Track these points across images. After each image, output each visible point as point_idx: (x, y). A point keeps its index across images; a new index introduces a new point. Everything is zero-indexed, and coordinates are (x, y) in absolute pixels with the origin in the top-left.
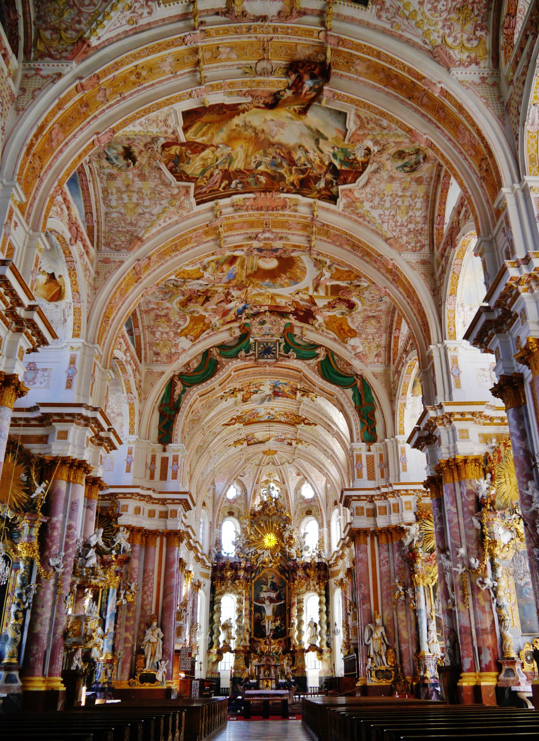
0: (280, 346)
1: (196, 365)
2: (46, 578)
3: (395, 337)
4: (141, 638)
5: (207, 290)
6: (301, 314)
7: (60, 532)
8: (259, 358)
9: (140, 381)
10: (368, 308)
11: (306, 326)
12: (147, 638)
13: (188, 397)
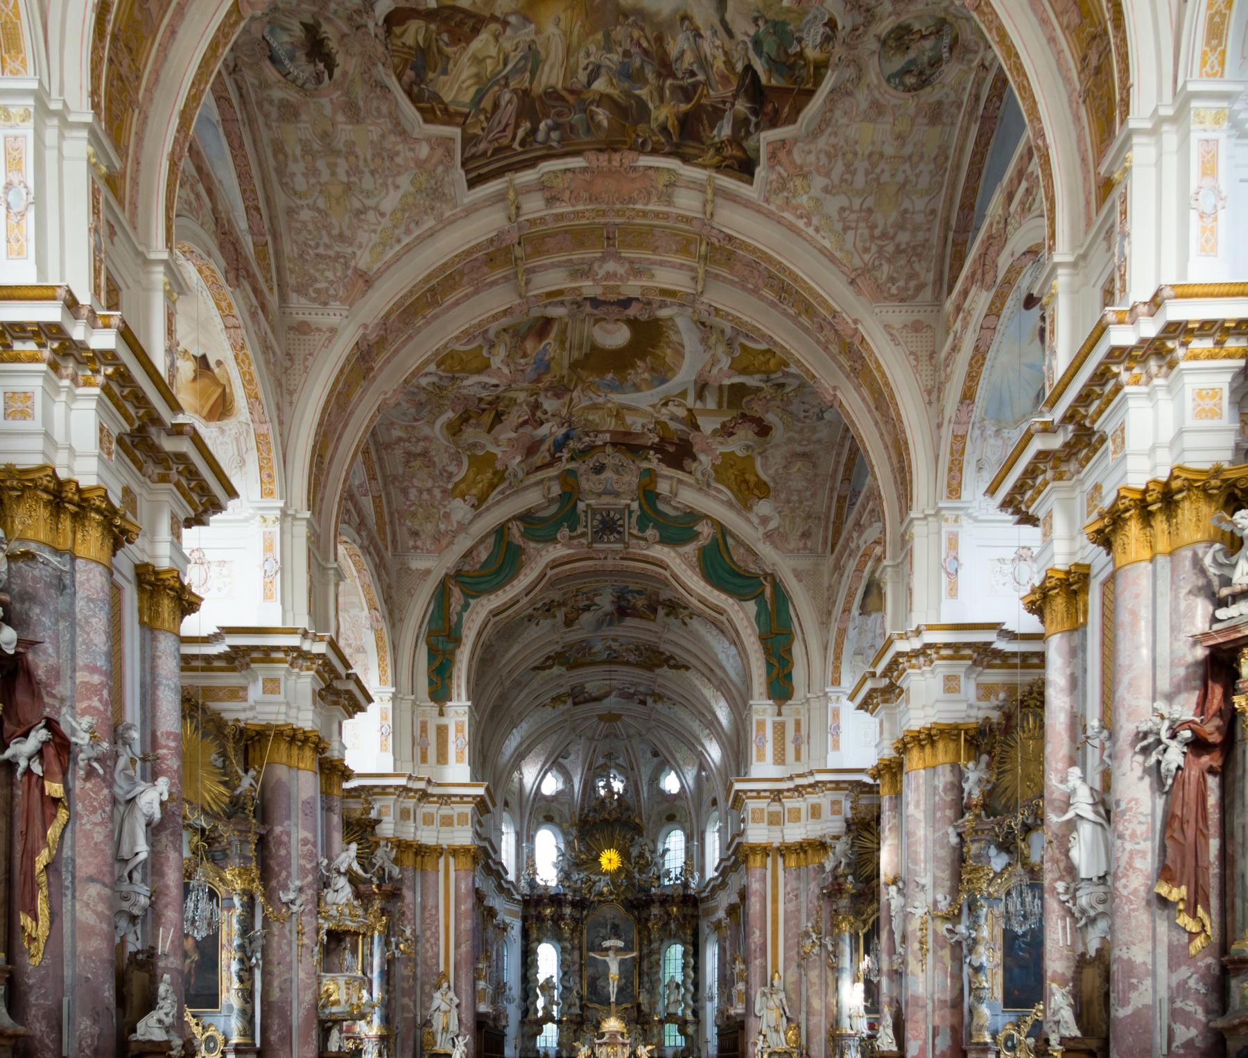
0: (630, 516)
1: (484, 556)
3: (839, 497)
4: (427, 1004)
5: (498, 398)
6: (671, 449)
8: (594, 541)
9: (389, 587)
10: (796, 436)
11: (680, 475)
13: (474, 616)
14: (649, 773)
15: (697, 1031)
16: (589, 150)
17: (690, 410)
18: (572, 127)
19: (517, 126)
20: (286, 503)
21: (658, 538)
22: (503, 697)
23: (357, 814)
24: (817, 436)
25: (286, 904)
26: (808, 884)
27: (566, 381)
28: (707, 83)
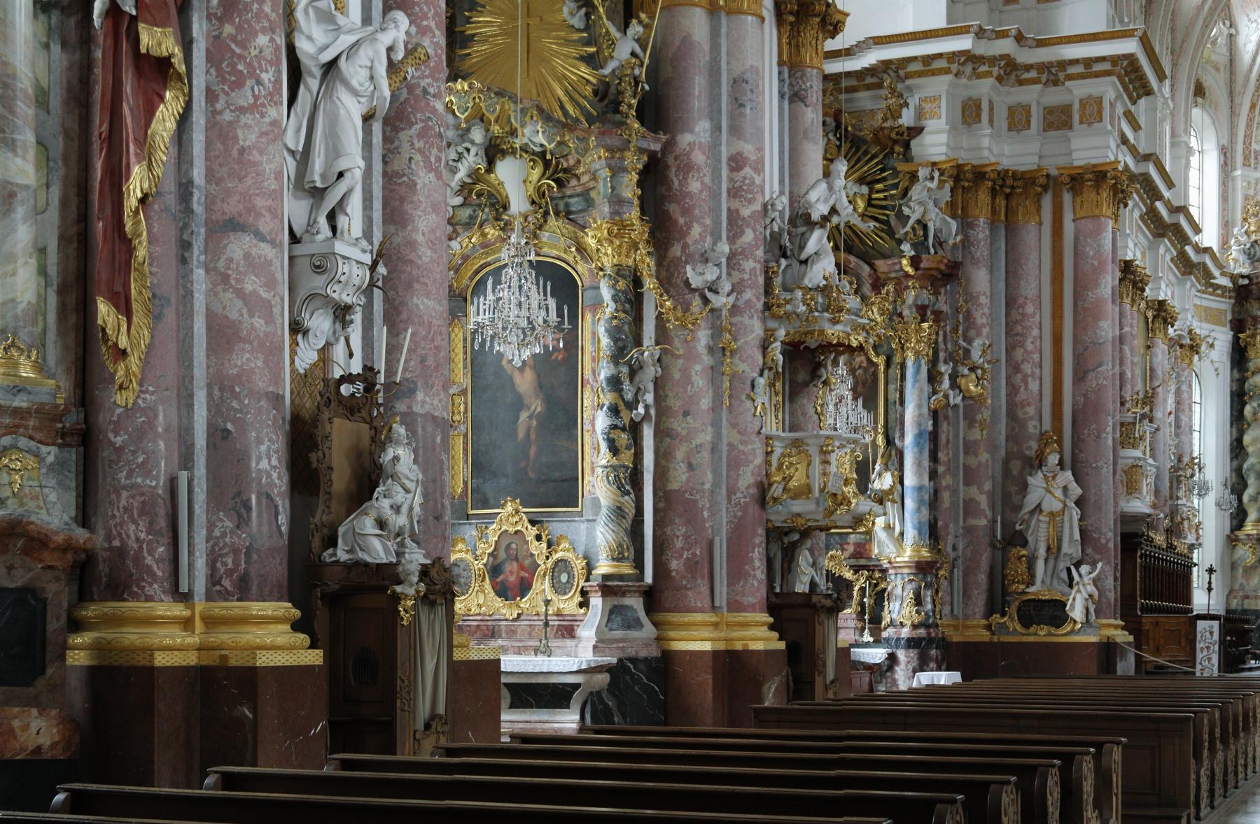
2: (684, 326)
7: (707, 180)
12: (1031, 500)
23: (878, 121)
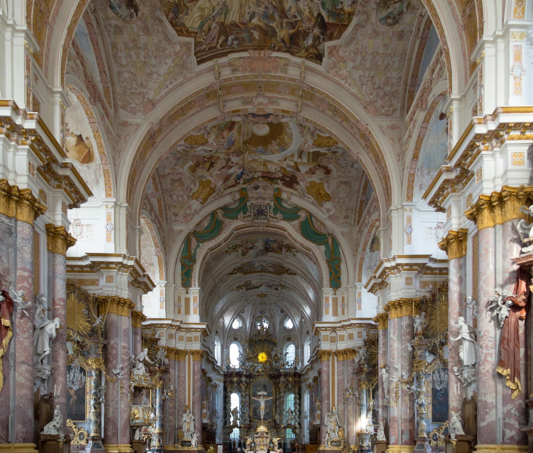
0: (270, 208)
1: (206, 225)
3: (361, 201)
4: (180, 419)
5: (212, 156)
6: (288, 179)
9: (164, 237)
10: (342, 174)
11: (291, 190)
13: (202, 251)
14: (279, 320)
15: (300, 432)
16: (251, 49)
17: (295, 163)
18: (243, 39)
19: (219, 38)
20: (117, 200)
21: (282, 218)
22: (215, 286)
23: (150, 336)
24: (351, 174)
25: (116, 375)
26: (348, 368)
27: (241, 149)
28: (302, 21)
